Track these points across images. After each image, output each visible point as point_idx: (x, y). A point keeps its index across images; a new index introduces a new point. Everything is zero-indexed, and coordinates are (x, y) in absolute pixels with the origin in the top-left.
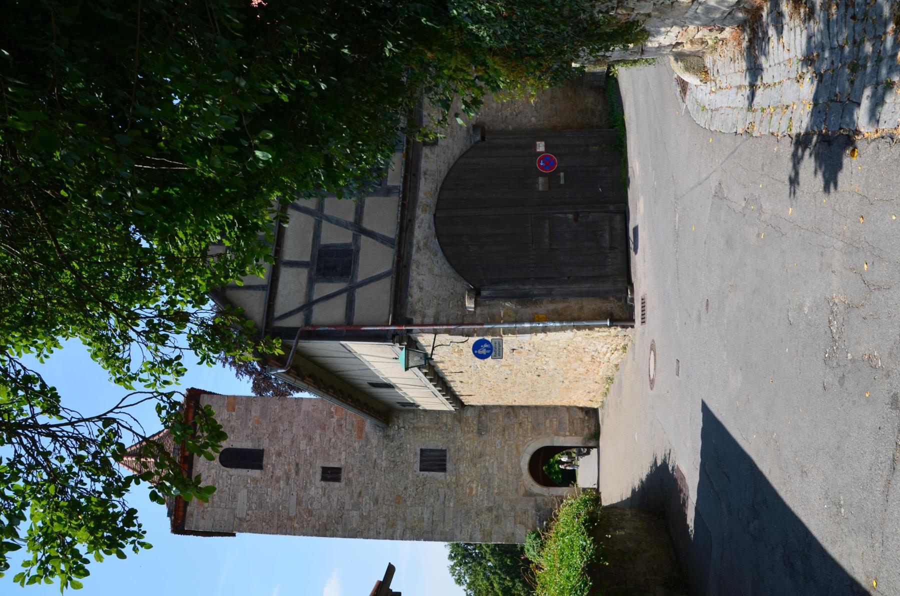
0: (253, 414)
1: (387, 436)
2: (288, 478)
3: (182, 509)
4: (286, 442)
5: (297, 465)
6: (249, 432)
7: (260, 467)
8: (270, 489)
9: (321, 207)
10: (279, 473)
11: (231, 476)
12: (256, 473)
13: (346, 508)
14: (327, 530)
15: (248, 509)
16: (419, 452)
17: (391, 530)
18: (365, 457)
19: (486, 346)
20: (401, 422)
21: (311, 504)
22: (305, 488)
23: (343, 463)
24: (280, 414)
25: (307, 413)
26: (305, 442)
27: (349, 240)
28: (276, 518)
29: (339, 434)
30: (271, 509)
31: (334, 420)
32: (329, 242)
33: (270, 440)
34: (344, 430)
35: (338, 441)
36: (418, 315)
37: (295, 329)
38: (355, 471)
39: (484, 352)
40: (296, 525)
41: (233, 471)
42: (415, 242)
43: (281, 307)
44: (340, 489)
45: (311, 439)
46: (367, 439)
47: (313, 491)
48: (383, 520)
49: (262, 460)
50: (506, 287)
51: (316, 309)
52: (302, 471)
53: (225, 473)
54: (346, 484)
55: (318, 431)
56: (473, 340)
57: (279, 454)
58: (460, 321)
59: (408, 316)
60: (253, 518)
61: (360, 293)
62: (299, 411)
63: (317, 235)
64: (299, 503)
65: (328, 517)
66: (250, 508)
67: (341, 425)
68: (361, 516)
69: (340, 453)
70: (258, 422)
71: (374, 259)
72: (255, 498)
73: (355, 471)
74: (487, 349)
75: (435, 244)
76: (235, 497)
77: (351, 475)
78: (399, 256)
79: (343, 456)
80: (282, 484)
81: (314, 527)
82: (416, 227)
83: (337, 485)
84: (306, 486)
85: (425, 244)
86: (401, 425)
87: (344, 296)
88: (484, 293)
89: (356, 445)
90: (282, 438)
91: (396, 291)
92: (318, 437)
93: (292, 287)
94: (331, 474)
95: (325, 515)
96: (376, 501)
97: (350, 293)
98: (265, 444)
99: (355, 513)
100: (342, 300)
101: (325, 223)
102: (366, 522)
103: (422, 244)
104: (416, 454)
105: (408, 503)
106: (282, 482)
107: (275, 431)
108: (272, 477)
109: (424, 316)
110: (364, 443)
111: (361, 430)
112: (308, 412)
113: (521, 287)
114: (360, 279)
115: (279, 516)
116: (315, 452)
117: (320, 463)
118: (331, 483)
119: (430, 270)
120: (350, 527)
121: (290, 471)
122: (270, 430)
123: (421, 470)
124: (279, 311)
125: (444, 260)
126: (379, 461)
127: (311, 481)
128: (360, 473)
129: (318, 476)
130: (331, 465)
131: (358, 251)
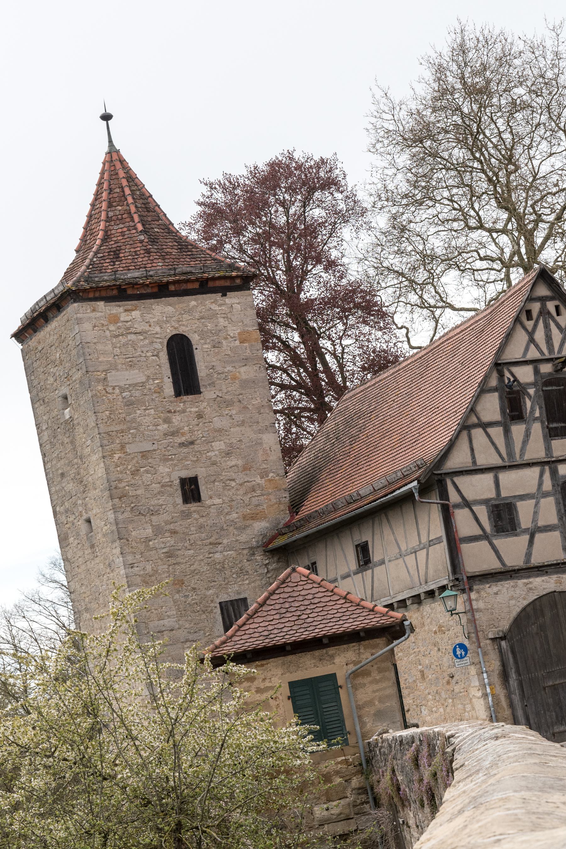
0: (243, 370)
1: (252, 550)
2: (173, 434)
3: (97, 294)
4: (218, 423)
5: (192, 443)
6: (219, 369)
7: (178, 394)
8: (152, 412)
9: (546, 495)
10: (176, 420)
12: (169, 389)
13: (153, 518)
14: (120, 498)
15: (120, 387)
16: (242, 596)
17: (138, 580)
18: (222, 529)
19: (463, 653)
20: (274, 566)
21: (147, 472)
22: (165, 459)
23: (209, 502)
24: (250, 407)
25: (259, 443)
26: (223, 447)
27: (523, 526)
28: (118, 428)
29: (241, 492)
30: (128, 418)
31: (258, 480)
32: (519, 509)
34: (250, 496)
35: (233, 491)
36: (477, 595)
37: (448, 499)
39: (458, 653)
41: (164, 357)
42: (531, 580)
43: (462, 482)
44: (175, 505)
45: (228, 454)
46: (245, 527)
47: (163, 469)
48: (149, 568)
49: (187, 393)
50: (511, 660)
51: (466, 511)
52: (186, 450)
53: (158, 346)
54: (183, 512)
55: (240, 462)
56: (466, 643)
57: (200, 416)
58: (479, 629)
59: (475, 587)
61: (484, 544)
62: (260, 431)
63: (522, 497)
64: (144, 455)
65: (137, 496)
66: (123, 390)
67: (254, 491)
68: (148, 540)
69: (219, 496)
70: (234, 378)
71: (513, 549)
72: (137, 394)
73: (201, 520)
74: (461, 654)
75: (532, 597)
76: (131, 366)
77: (196, 516)
78: (518, 570)
79: (217, 501)
80: (164, 427)
81: (120, 480)
82: (543, 578)
83: (179, 500)
84: (168, 460)
85: (531, 589)
86: (270, 567)
87: (479, 532)
88: (503, 643)
89: (235, 515)
91: (491, 574)
92: (233, 463)
93: (478, 487)
94: (190, 490)
95: (139, 492)
96: (170, 555)
97: (485, 536)
98: (208, 393)
99: (149, 531)
100: (478, 531)
101: (533, 501)
102: (142, 547)
103: (530, 586)
104: (239, 593)
105: (177, 596)
106: (166, 426)
107: (229, 404)
108: (170, 412)
109: (477, 600)
110: (238, 525)
111: (254, 517)
112: (261, 444)
113: (513, 670)
114: (495, 542)
116: (214, 464)
117: (201, 472)
118: (179, 492)
119: (512, 598)
120: (130, 528)
121: (183, 434)
122: (228, 397)
123: (220, 603)
124: (459, 480)
125: (522, 606)
126: (220, 548)
127: (175, 465)
128: (201, 527)
129: (185, 474)
130: (202, 488)
131: (516, 535)
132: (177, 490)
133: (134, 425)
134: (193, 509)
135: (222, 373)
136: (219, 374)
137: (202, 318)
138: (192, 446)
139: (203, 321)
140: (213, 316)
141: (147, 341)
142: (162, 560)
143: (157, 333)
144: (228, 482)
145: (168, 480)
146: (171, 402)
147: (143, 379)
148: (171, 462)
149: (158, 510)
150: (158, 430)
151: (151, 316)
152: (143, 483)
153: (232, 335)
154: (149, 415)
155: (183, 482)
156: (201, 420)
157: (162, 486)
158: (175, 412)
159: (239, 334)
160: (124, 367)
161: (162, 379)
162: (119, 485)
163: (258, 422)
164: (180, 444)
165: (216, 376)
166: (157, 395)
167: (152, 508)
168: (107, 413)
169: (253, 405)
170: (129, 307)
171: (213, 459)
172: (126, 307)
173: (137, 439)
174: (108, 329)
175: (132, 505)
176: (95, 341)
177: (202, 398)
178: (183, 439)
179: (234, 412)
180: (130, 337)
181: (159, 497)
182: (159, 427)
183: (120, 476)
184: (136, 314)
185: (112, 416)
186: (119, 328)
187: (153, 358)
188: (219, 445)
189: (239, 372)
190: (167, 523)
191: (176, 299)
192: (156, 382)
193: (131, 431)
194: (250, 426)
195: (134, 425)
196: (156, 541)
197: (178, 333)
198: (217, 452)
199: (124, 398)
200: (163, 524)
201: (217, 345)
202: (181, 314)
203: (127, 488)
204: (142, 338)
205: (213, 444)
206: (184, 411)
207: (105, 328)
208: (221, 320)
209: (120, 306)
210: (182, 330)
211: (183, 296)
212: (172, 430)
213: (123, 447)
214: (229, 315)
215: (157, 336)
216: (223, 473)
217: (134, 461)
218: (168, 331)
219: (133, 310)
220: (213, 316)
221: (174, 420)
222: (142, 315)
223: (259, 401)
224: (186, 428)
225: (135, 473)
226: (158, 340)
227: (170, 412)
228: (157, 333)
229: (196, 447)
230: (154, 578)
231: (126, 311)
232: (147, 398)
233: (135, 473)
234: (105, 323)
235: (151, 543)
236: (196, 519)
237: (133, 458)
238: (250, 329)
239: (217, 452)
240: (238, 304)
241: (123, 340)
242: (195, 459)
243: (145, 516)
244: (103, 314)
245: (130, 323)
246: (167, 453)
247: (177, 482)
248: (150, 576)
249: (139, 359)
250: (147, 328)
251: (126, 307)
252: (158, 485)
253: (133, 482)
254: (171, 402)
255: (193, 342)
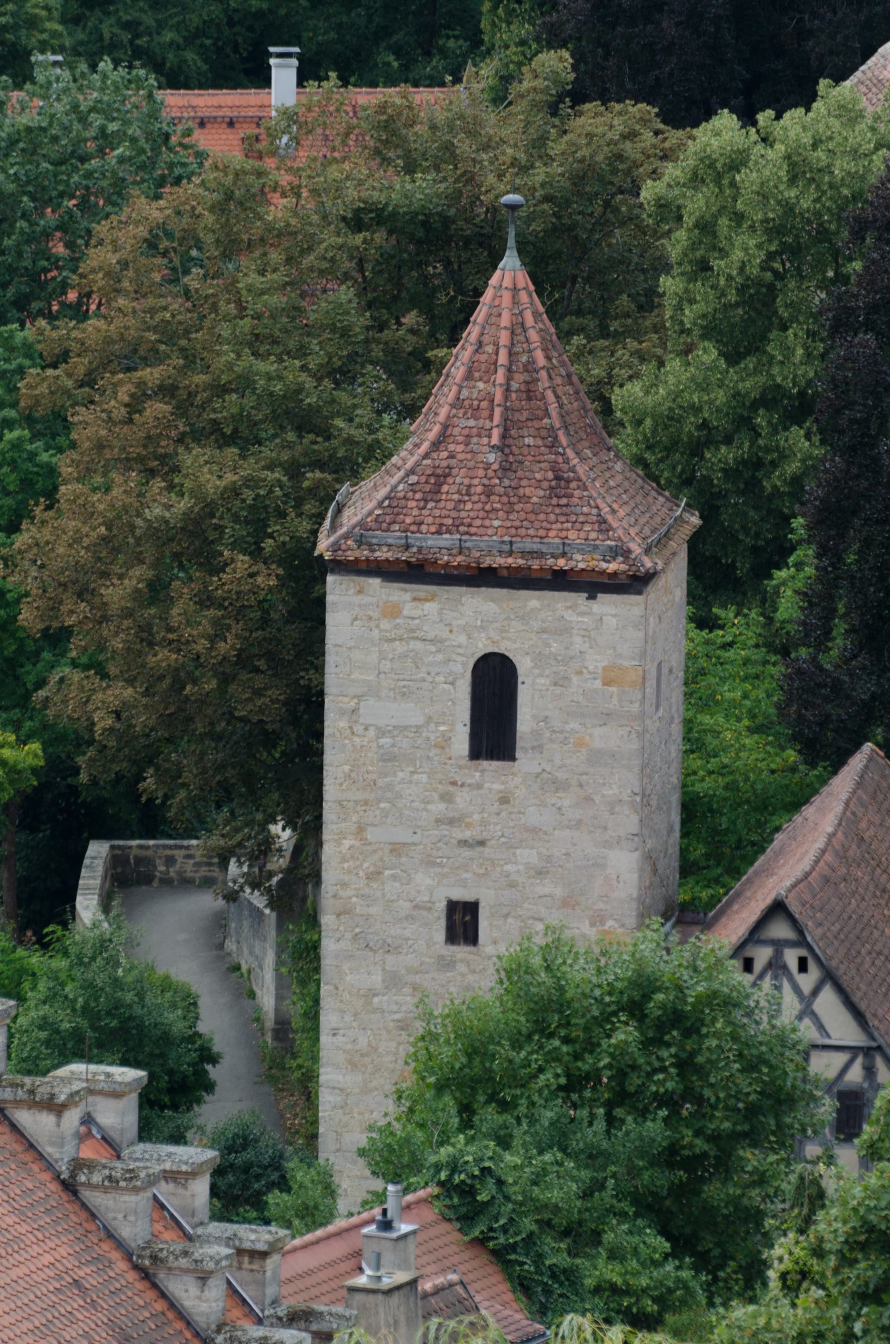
0: (598, 731)
2: (451, 822)
4: (535, 817)
5: (482, 843)
7: (476, 754)
8: (424, 778)
10: (462, 798)
11: (452, 684)
12: (461, 743)
13: (390, 958)
14: (338, 915)
15: (378, 728)
21: (394, 878)
22: (429, 862)
28: (360, 796)
30: (380, 782)
33: (537, 775)
38: (471, 978)
40: (347, 843)
45: (541, 873)
47: (423, 880)
48: (363, 1042)
52: (466, 853)
53: (457, 668)
54: (441, 957)
55: (559, 892)
57: (504, 800)
60: (357, 740)
62: (607, 844)
64: (397, 849)
65: (368, 917)
66: (382, 732)
68: (372, 993)
70: (580, 744)
73: (471, 978)
81: (344, 885)
90: (543, 804)
92: (546, 891)
94: (462, 922)
95: (373, 910)
98: (526, 761)
99: (377, 979)
106: (442, 806)
107: (560, 786)
108: (454, 783)
115: (366, 803)
116: (513, 885)
118: (442, 923)
120: (345, 967)
121: (469, 825)
122: (561, 775)
132: (439, 918)
133: (388, 795)
134: (459, 956)
135: (561, 732)
136: (554, 732)
137: (544, 631)
138: (481, 849)
139: (545, 636)
140: (564, 630)
141: (440, 657)
142: (389, 1032)
143: (459, 646)
144: (530, 922)
145: (426, 899)
146: (460, 767)
147: (420, 720)
148: (438, 870)
149: (400, 946)
150: (428, 811)
151: (455, 614)
152: (384, 895)
153: (591, 668)
154: (417, 783)
155: (453, 907)
156: (504, 807)
157: (416, 907)
158: (462, 785)
159: (605, 669)
160: (391, 694)
161: (453, 724)
162: (342, 893)
163: (605, 828)
164: (460, 842)
165: (547, 735)
166: (438, 751)
167: (389, 941)
168: (347, 768)
169: (603, 796)
170: (422, 595)
171: (512, 877)
172: (416, 594)
173: (389, 821)
174: (377, 626)
175: (357, 930)
176: (352, 643)
177: (514, 770)
178: (467, 834)
179: (566, 802)
180: (413, 644)
181: (405, 924)
182: (430, 807)
183: (346, 878)
184: (431, 608)
185: (353, 775)
186: (397, 627)
187: (446, 686)
188: (528, 856)
189: (591, 736)
190: (410, 970)
191: (504, 592)
192: (442, 728)
193: (382, 805)
194: (590, 832)
195: (388, 795)
196: (385, 998)
197: (496, 650)
198: (521, 868)
199: (379, 747)
200: (403, 972)
201: (561, 682)
202: (508, 618)
203: (354, 899)
204: (433, 649)
205: (518, 851)
206: (479, 786)
207: (373, 624)
208: (578, 640)
209: (406, 591)
210: (503, 647)
211: (518, 589)
212: (451, 815)
213: (361, 829)
214: (593, 634)
215: (460, 651)
216: (526, 905)
217: (376, 857)
218: (480, 645)
219: (427, 600)
220: (564, 630)
221: (458, 799)
222: (440, 612)
223: (616, 791)
224: (476, 817)
225: (374, 875)
226: (459, 659)
227: (454, 783)
228: (459, 646)
229: (487, 851)
230: (367, 1060)
231: (415, 599)
232: (419, 753)
233: (374, 875)
234: (376, 615)
235: (376, 1000)
236: (463, 975)
237: (374, 852)
238: (626, 663)
239: (521, 868)
240: (614, 616)
241: (399, 647)
242: (482, 871)
243: (375, 952)
244: (374, 600)
245: (417, 622)
246: (434, 853)
247: (442, 905)
248: (362, 1055)
249: (419, 685)
250: (445, 634)
251: (416, 594)
252: (408, 905)
253: (367, 891)
254: (460, 767)
255: (521, 671)
